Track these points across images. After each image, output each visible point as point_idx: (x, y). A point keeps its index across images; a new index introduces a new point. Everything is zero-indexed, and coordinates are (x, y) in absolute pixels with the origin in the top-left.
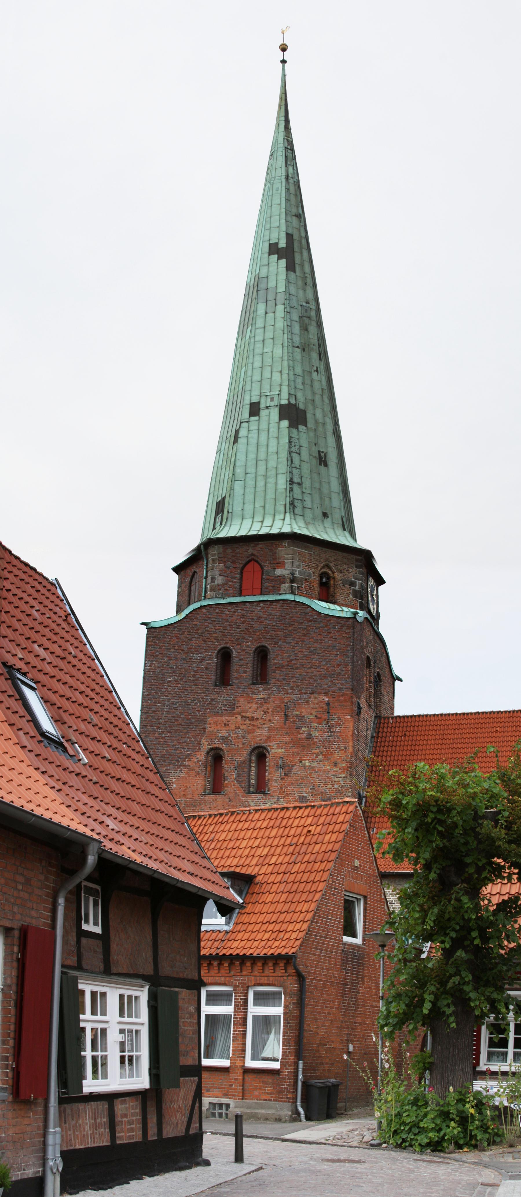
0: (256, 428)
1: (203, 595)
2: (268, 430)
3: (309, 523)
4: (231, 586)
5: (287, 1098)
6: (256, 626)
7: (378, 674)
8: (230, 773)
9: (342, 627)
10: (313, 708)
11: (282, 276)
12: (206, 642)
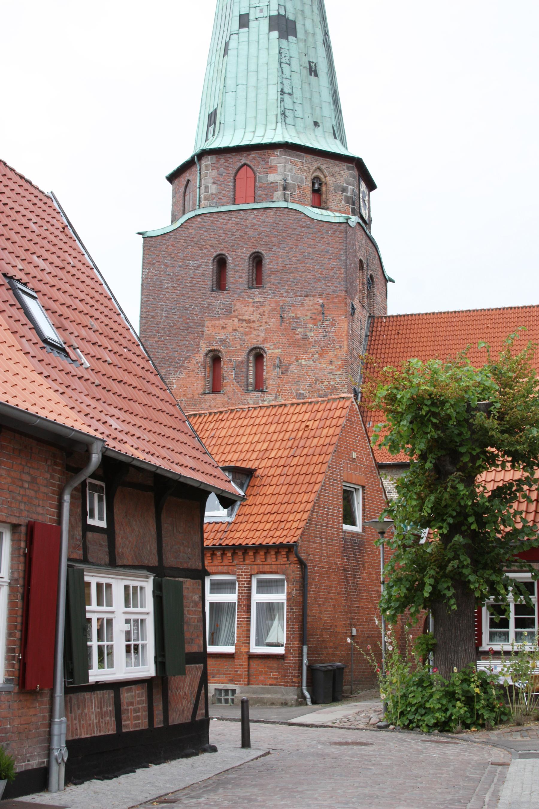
0: (247, 39)
1: (197, 204)
4: (224, 195)
5: (293, 682)
6: (251, 233)
7: (371, 276)
8: (228, 371)
9: (334, 232)
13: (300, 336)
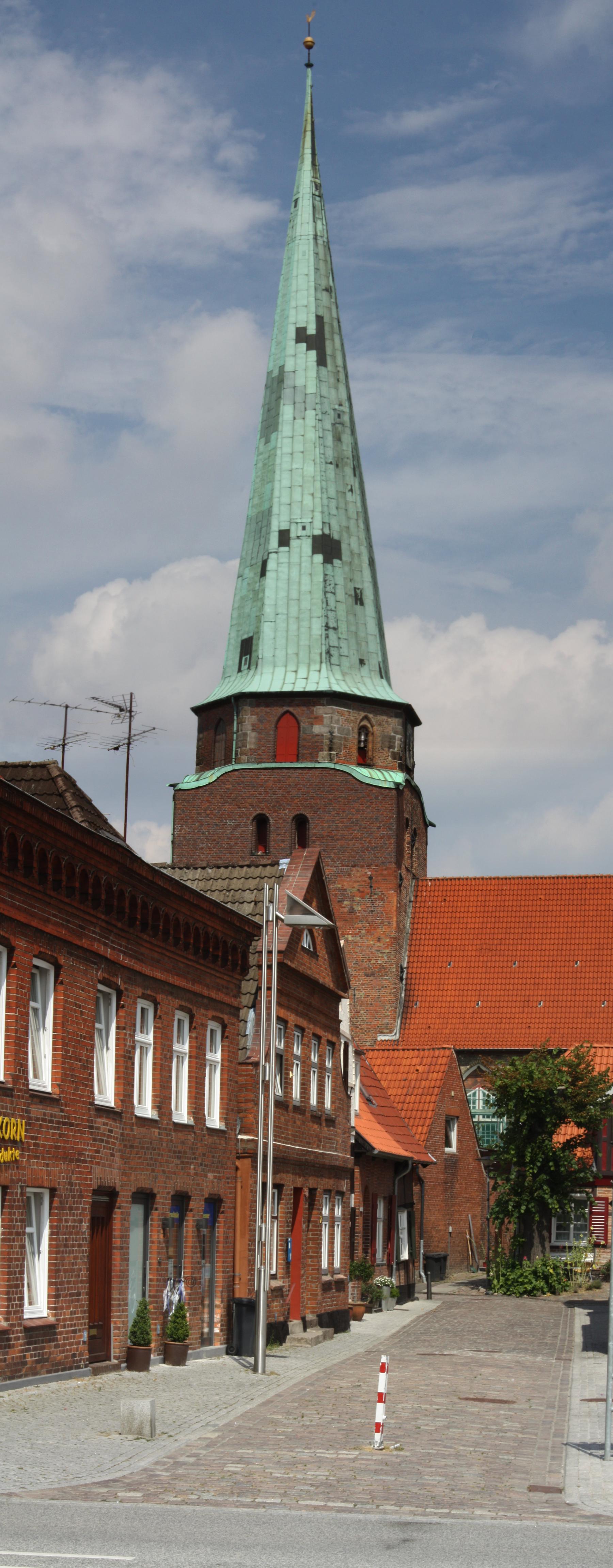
2: (300, 565)
3: (346, 673)
6: (294, 792)
10: (355, 882)
11: (312, 373)
12: (240, 808)
13: (346, 910)
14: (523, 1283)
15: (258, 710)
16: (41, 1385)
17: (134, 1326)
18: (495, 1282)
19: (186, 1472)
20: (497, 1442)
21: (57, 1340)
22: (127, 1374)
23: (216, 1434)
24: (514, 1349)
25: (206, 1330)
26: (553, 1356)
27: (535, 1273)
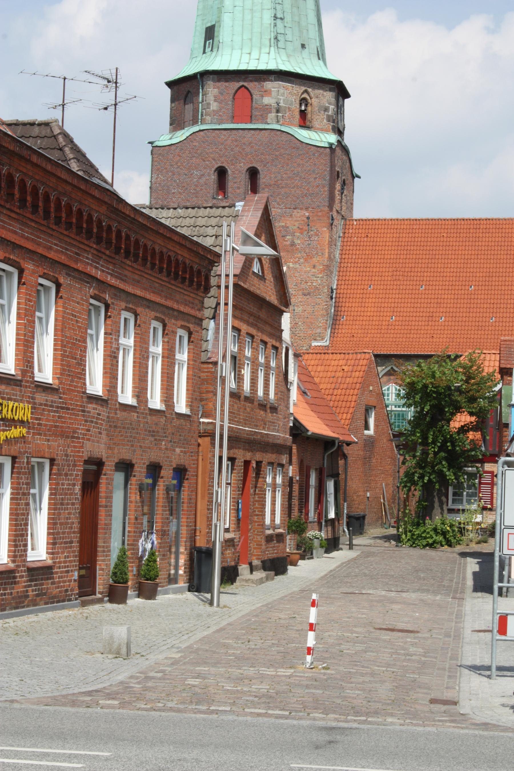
10: (296, 221)
12: (204, 161)
13: (288, 243)
14: (425, 538)
15: (219, 84)
16: (40, 614)
17: (115, 568)
18: (404, 536)
19: (154, 685)
20: (405, 664)
21: (53, 578)
22: (109, 606)
23: (179, 655)
24: (418, 590)
25: (172, 572)
26: (449, 595)
27: (435, 530)
